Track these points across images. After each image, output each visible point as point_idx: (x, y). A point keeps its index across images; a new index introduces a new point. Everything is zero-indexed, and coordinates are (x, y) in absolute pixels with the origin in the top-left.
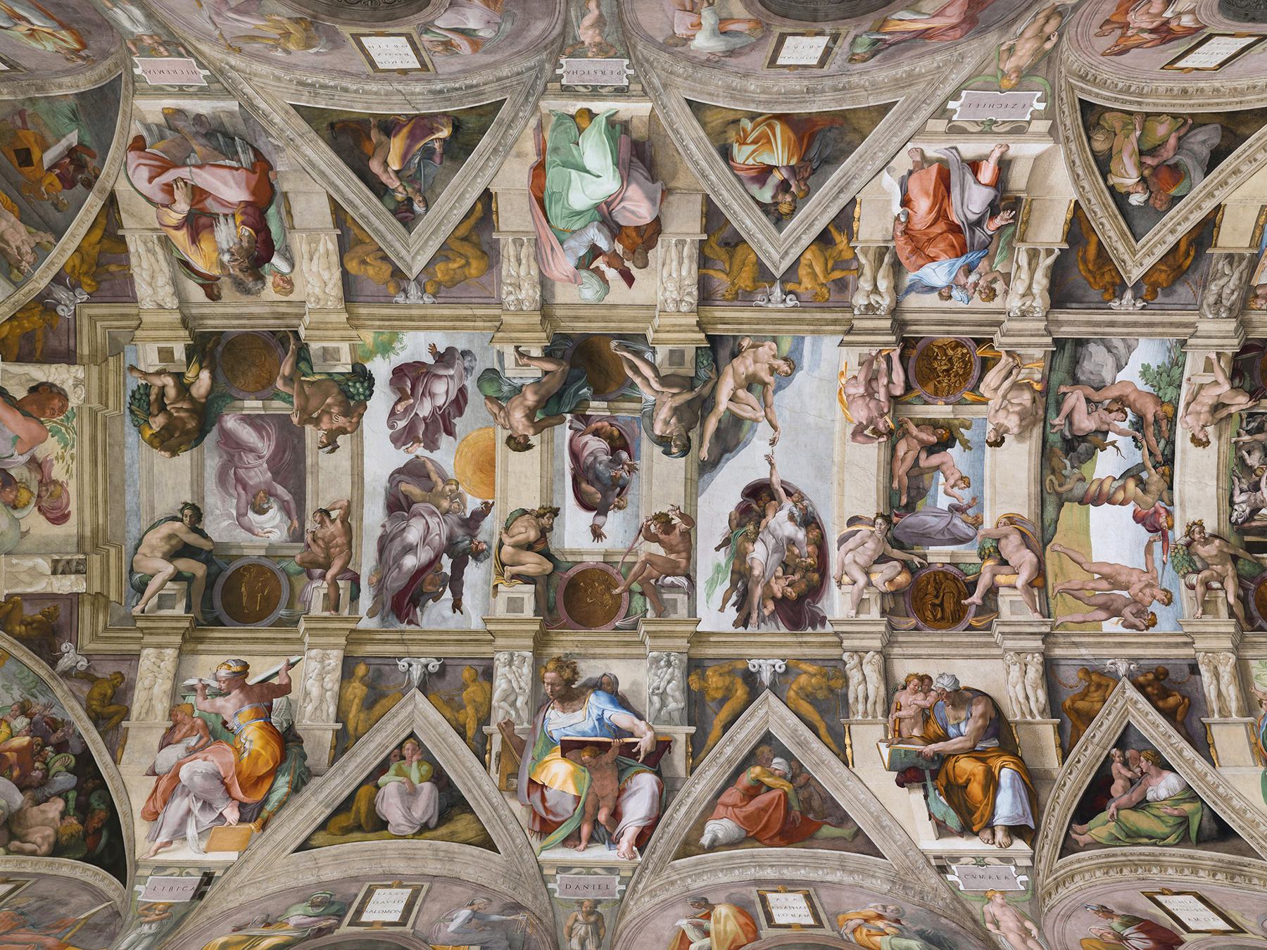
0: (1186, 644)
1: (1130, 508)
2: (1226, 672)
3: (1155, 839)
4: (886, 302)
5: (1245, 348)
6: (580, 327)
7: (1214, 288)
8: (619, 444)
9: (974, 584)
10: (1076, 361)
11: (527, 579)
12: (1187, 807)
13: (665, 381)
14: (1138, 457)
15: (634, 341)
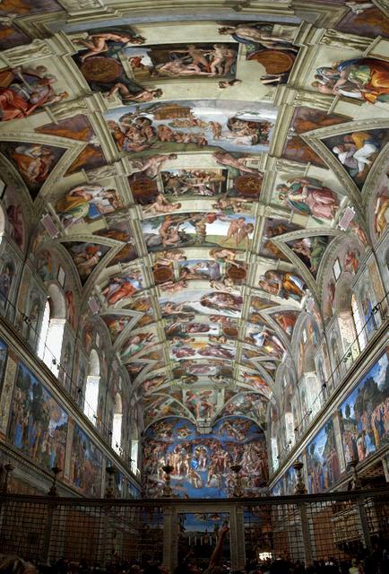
0: (261, 218)
1: (207, 224)
2: (273, 211)
3: (322, 251)
4: (146, 291)
5: (139, 203)
6: (164, 337)
7: (119, 221)
8: (192, 326)
9: (233, 265)
10: (155, 246)
11: (225, 340)
12: (316, 240)
13: (175, 322)
14: (187, 223)
15: (165, 329)
